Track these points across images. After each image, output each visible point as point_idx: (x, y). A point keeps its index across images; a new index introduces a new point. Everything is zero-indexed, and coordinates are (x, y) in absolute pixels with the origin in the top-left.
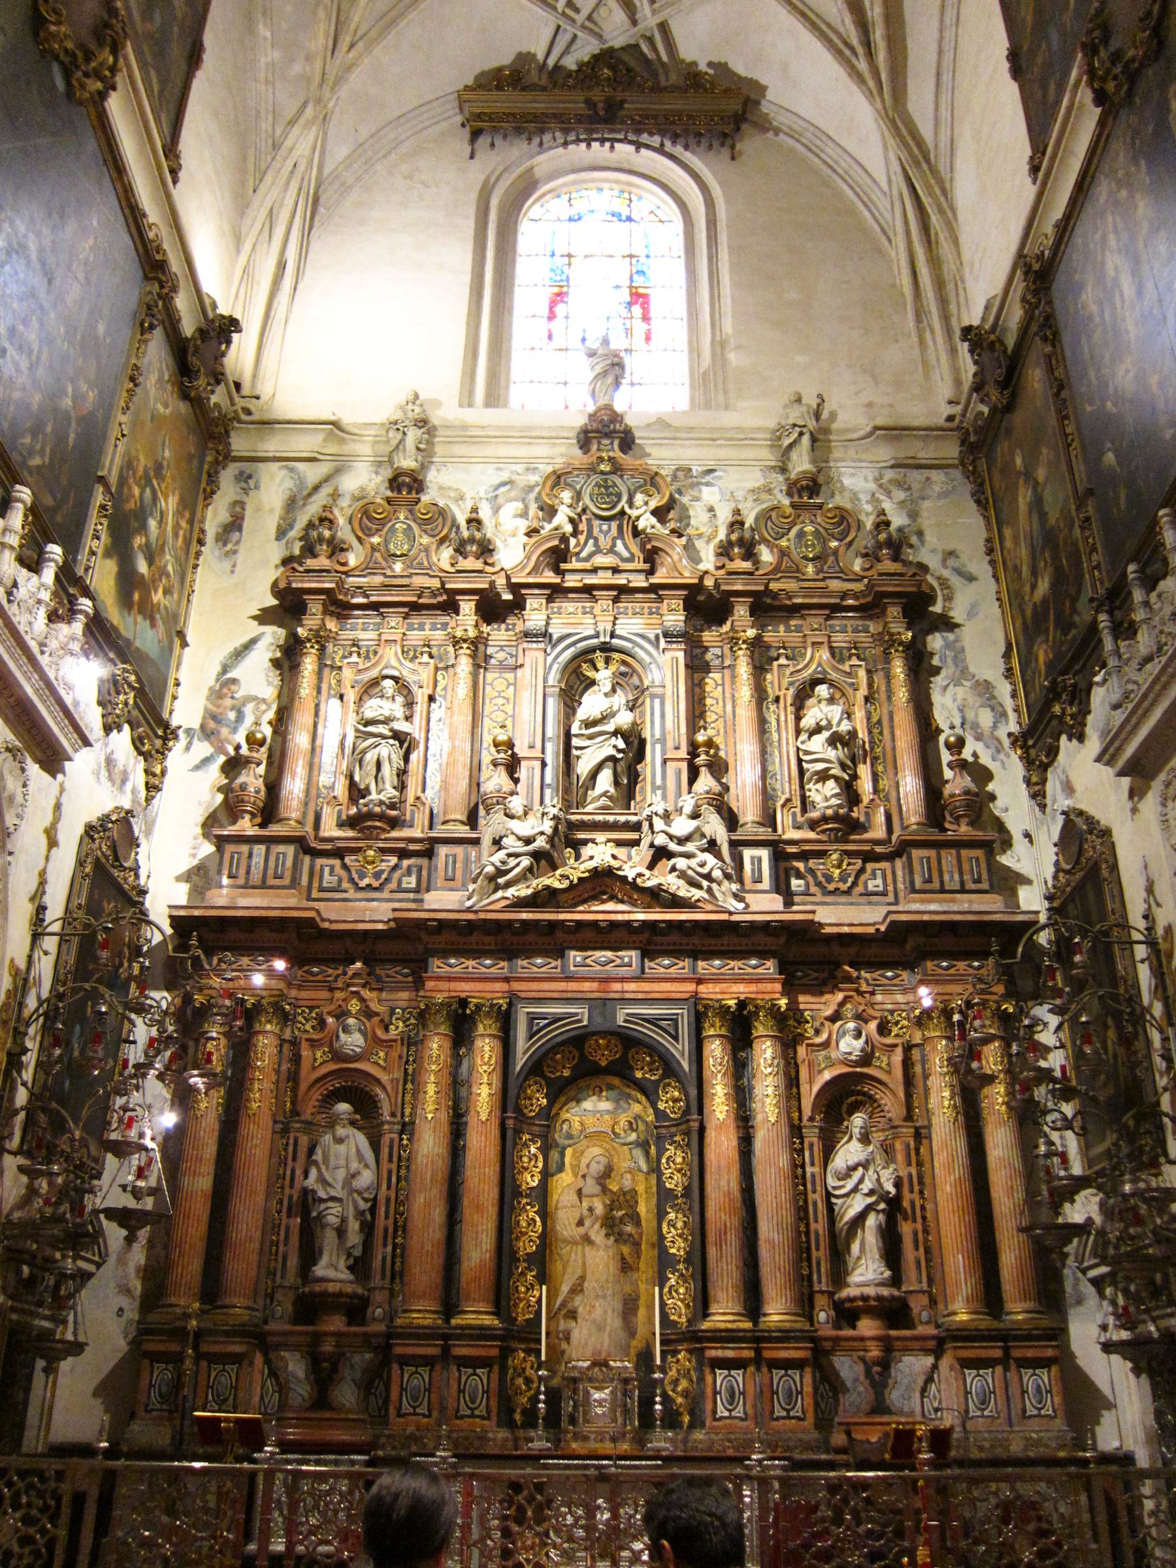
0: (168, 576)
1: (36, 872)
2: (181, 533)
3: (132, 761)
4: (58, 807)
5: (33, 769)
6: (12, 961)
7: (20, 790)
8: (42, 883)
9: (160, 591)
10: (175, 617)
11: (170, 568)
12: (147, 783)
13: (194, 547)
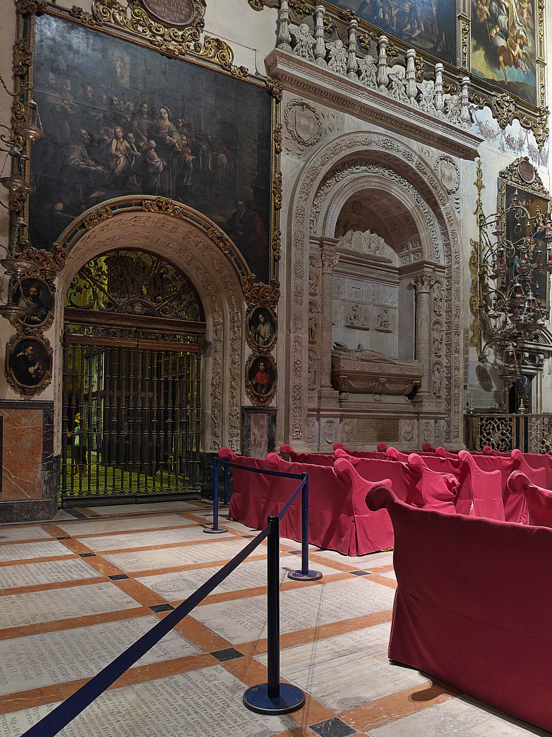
0: (521, 37)
1: (475, 202)
2: (525, 11)
3: (524, 134)
4: (479, 171)
5: (460, 162)
6: (471, 240)
7: (454, 173)
8: (479, 204)
9: (518, 47)
10: (533, 55)
11: (522, 33)
12: (537, 141)
13: (537, 11)
